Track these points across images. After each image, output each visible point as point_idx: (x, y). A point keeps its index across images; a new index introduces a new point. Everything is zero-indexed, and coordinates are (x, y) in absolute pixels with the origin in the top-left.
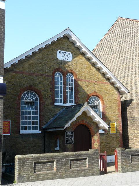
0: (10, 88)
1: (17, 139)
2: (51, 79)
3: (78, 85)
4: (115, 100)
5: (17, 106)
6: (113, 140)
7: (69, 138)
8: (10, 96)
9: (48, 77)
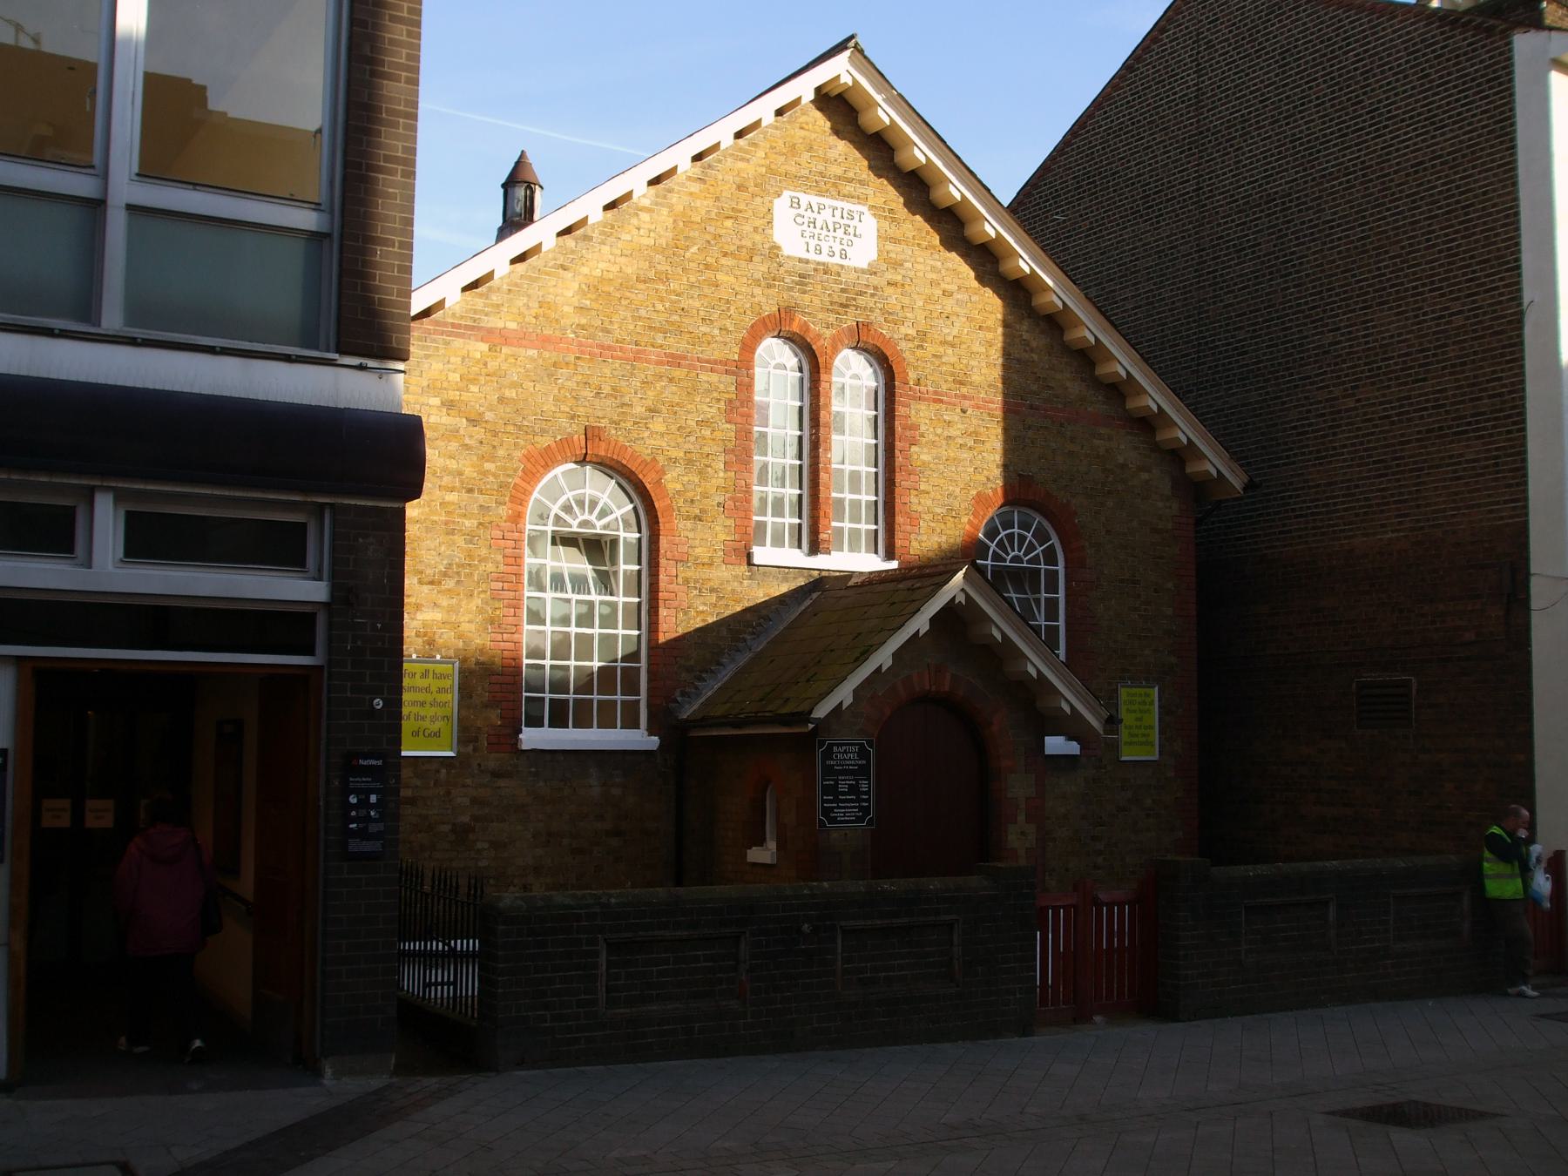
0: (454, 446)
5: (502, 568)
7: (843, 787)
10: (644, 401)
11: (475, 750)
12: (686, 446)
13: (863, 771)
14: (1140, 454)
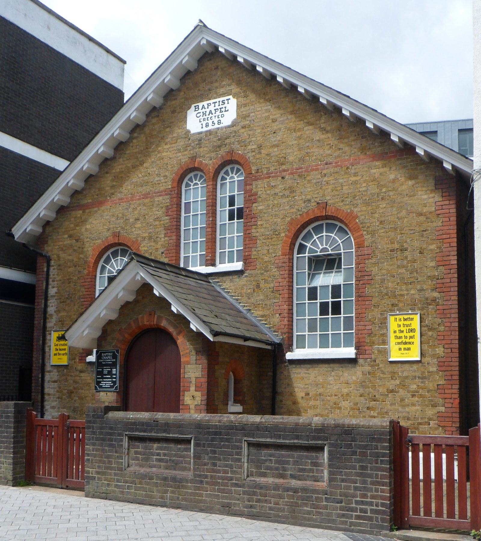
0: (71, 251)
1: (82, 375)
2: (166, 200)
4: (422, 218)
5: (85, 293)
6: (403, 385)
7: (105, 372)
8: (71, 270)
10: (134, 217)
11: (75, 362)
12: (149, 231)
13: (114, 365)
14: (408, 169)
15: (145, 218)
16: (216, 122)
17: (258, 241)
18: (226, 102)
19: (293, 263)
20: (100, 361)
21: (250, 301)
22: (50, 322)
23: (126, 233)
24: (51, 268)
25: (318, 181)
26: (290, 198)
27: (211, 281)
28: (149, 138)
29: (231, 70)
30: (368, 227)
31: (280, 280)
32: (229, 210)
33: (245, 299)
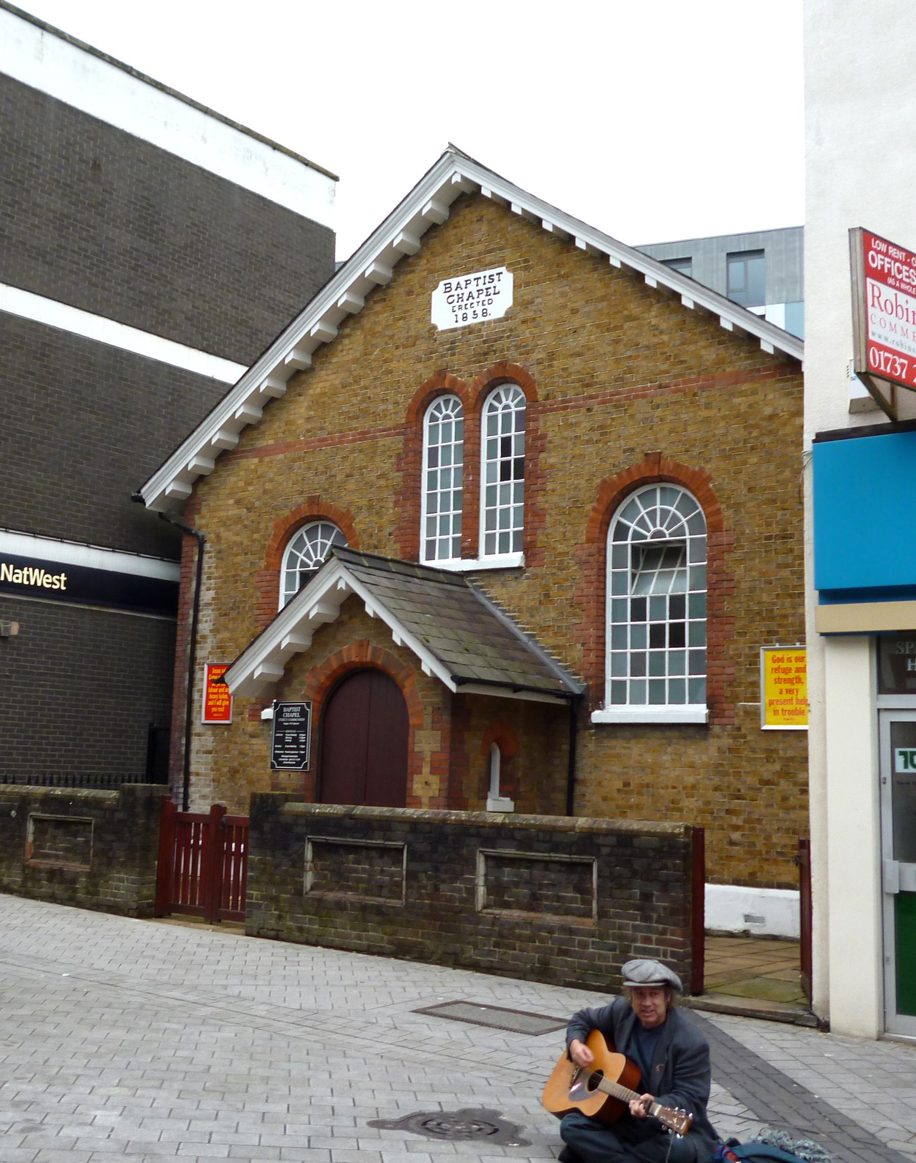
2: (396, 443)
3: (539, 443)
5: (261, 600)
7: (288, 739)
9: (388, 436)
11: (242, 719)
12: (369, 496)
13: (302, 727)
15: (362, 474)
16: (479, 312)
17: (548, 518)
18: (496, 278)
19: (605, 556)
20: (281, 720)
21: (533, 620)
22: (202, 648)
23: (331, 498)
24: (206, 557)
25: (646, 415)
26: (601, 445)
27: (469, 584)
28: (369, 337)
29: (503, 224)
30: (729, 498)
31: (584, 585)
32: (502, 463)
33: (526, 618)
